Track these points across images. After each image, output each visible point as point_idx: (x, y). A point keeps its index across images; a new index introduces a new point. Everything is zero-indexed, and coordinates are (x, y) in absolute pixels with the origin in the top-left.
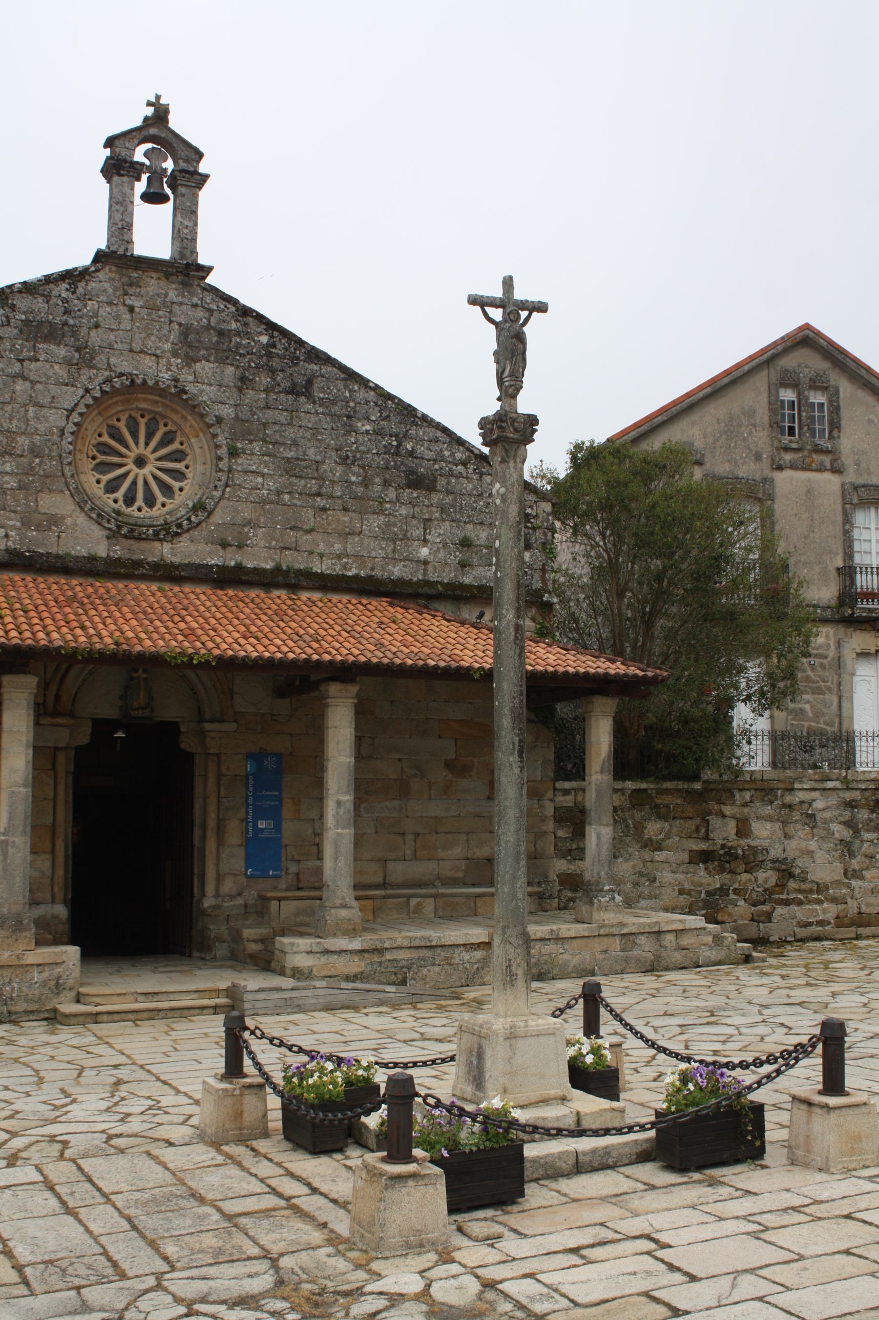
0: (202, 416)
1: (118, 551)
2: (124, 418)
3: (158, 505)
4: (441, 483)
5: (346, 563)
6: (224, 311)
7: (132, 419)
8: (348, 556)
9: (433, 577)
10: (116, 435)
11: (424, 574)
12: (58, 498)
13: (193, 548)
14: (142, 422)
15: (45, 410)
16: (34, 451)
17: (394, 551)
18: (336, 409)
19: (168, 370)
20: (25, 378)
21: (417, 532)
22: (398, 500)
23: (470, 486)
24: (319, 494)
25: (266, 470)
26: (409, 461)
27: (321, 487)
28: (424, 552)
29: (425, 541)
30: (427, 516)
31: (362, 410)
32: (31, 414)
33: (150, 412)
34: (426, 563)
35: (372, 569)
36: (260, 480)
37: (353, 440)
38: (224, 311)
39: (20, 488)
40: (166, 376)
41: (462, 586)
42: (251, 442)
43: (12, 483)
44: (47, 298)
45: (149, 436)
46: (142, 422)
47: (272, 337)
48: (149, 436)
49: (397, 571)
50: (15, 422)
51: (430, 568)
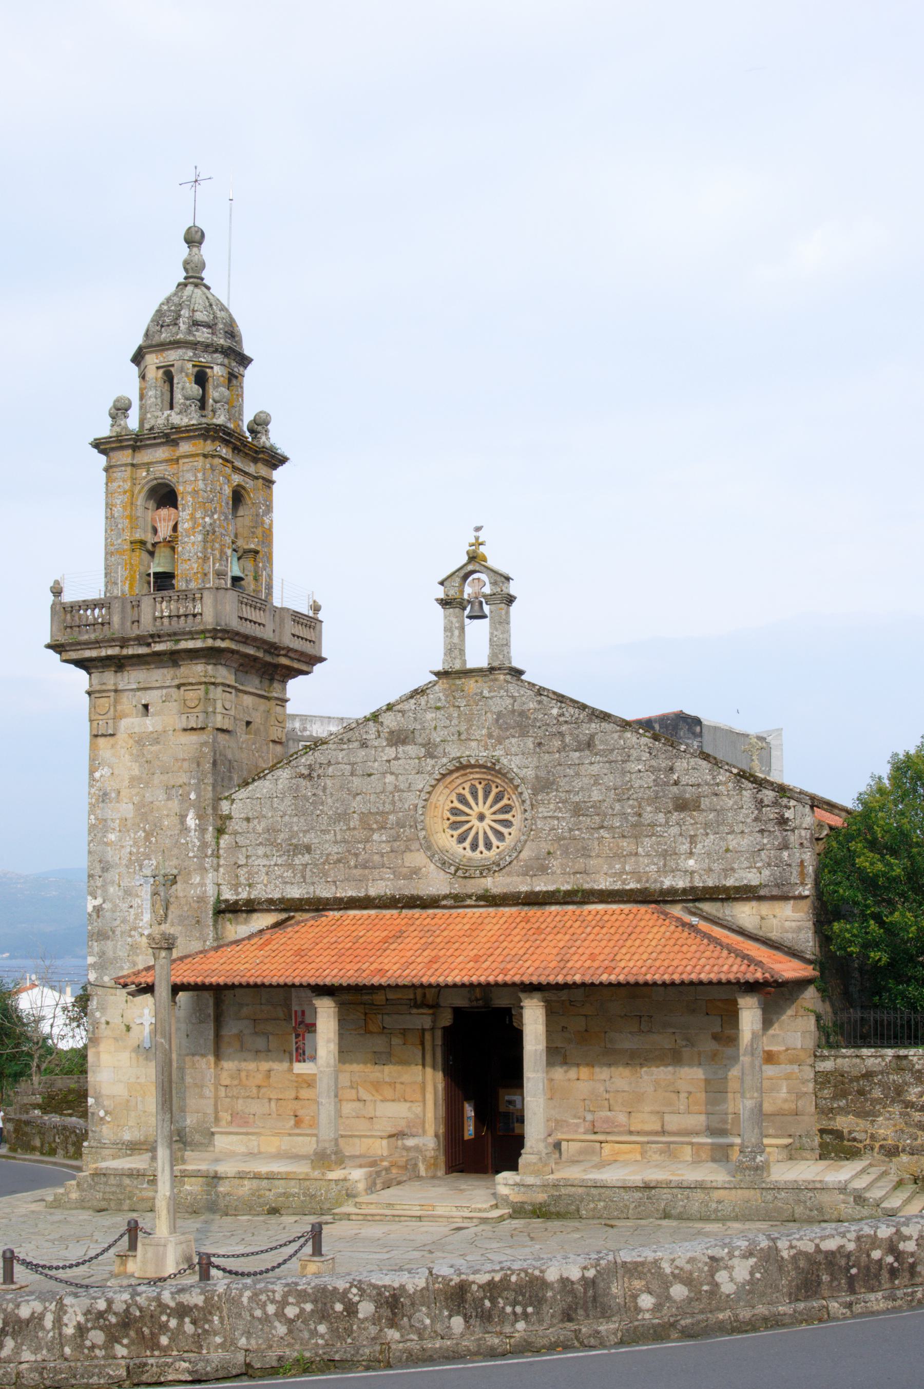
0: (511, 780)
1: (457, 889)
2: (467, 786)
3: (494, 848)
4: (705, 803)
5: (626, 879)
6: (523, 696)
7: (473, 786)
8: (627, 874)
9: (698, 883)
10: (462, 799)
11: (691, 881)
12: (416, 854)
13: (508, 880)
14: (480, 788)
15: (405, 794)
16: (400, 824)
17: (665, 865)
18: (612, 757)
19: (486, 749)
20: (392, 773)
21: (685, 847)
22: (667, 822)
23: (731, 802)
24: (602, 827)
25: (560, 815)
26: (675, 789)
27: (603, 821)
28: (691, 862)
29: (691, 853)
30: (692, 833)
31: (634, 754)
32: (397, 798)
33: (484, 779)
34: (692, 873)
35: (647, 881)
36: (556, 822)
37: (627, 779)
38: (523, 696)
39: (392, 851)
40: (485, 754)
41: (726, 889)
42: (548, 794)
43: (386, 848)
44: (403, 712)
45: (486, 797)
46: (480, 788)
47: (560, 708)
48: (486, 797)
49: (667, 883)
50: (387, 805)
51: (696, 876)
